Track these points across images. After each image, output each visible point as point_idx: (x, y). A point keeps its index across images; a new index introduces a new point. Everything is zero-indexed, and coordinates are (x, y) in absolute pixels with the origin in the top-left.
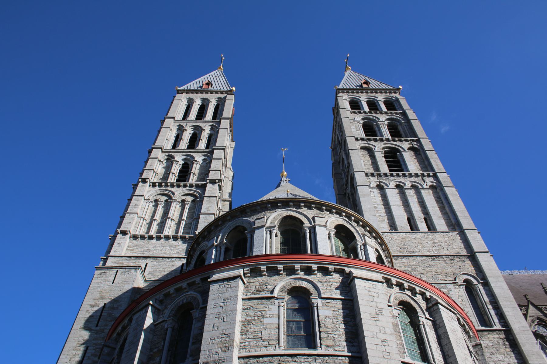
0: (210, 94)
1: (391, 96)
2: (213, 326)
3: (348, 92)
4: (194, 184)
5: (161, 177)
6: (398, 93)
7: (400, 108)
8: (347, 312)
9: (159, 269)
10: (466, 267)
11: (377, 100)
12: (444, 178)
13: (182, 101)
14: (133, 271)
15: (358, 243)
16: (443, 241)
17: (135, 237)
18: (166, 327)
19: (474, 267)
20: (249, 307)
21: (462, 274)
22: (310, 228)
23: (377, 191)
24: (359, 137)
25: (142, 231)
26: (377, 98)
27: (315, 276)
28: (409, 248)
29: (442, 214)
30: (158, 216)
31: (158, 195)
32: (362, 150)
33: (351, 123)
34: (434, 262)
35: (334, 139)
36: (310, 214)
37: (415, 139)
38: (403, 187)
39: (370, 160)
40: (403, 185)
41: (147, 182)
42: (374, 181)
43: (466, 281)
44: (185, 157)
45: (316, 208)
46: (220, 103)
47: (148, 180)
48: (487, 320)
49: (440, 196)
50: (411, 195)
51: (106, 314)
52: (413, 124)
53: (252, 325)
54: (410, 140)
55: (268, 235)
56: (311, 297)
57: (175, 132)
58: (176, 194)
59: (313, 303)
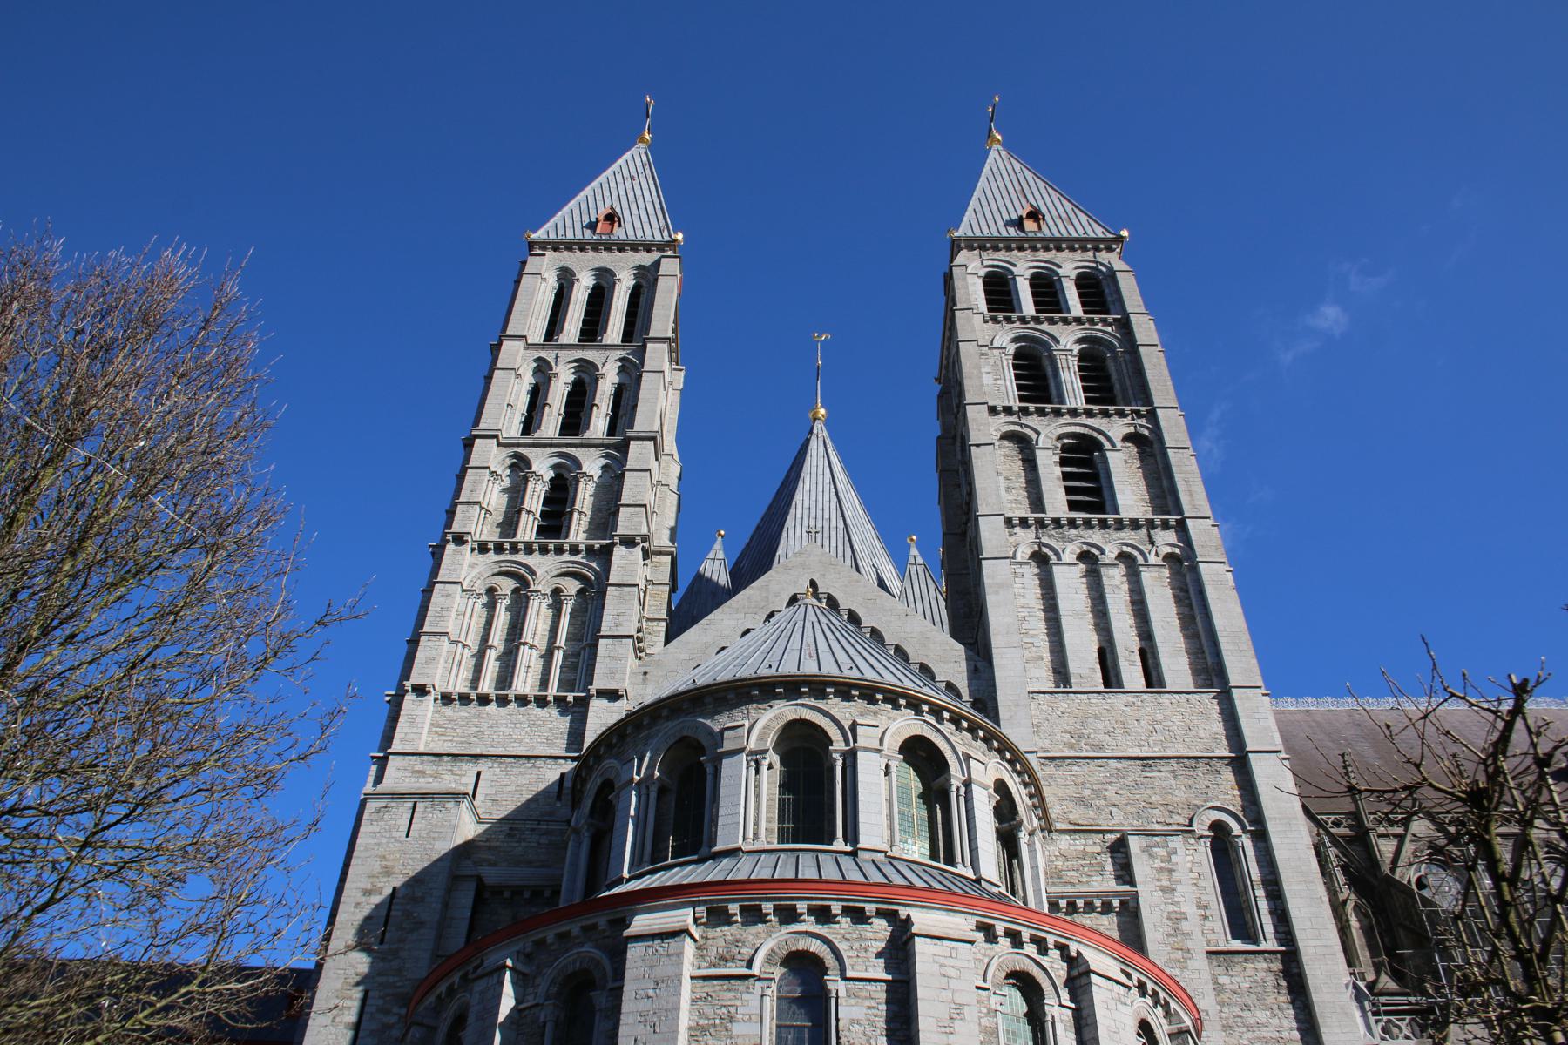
0: (617, 253)
1: (1097, 262)
2: (636, 1040)
3: (982, 248)
4: (582, 547)
5: (500, 519)
6: (1118, 250)
7: (1117, 304)
8: (896, 1008)
9: (509, 789)
10: (1222, 788)
11: (1057, 274)
12: (1205, 534)
13: (544, 280)
14: (451, 805)
15: (953, 781)
16: (1177, 719)
17: (447, 699)
18: (542, 1019)
19: (1240, 788)
20: (705, 995)
21: (1209, 808)
22: (844, 755)
23: (1031, 571)
24: (999, 404)
25: (460, 686)
26: (1060, 267)
27: (837, 926)
28: (1092, 736)
29: (1186, 637)
30: (498, 638)
31: (494, 575)
32: (1006, 443)
33: (982, 354)
34: (1149, 774)
35: (944, 362)
36: (847, 715)
37: (1143, 409)
38: (1098, 559)
39: (1023, 474)
40: (1097, 553)
41: (467, 541)
42: (1025, 541)
43: (1217, 827)
44: (556, 460)
45: (861, 696)
46: (644, 284)
47: (467, 537)
48: (1251, 924)
49: (1187, 585)
50: (1115, 580)
51: (399, 913)
52: (1145, 360)
53: (709, 1037)
54: (1132, 414)
55: (752, 771)
56: (826, 977)
57: (528, 380)
58: (539, 573)
59: (830, 991)
